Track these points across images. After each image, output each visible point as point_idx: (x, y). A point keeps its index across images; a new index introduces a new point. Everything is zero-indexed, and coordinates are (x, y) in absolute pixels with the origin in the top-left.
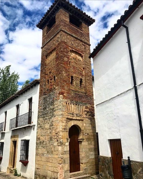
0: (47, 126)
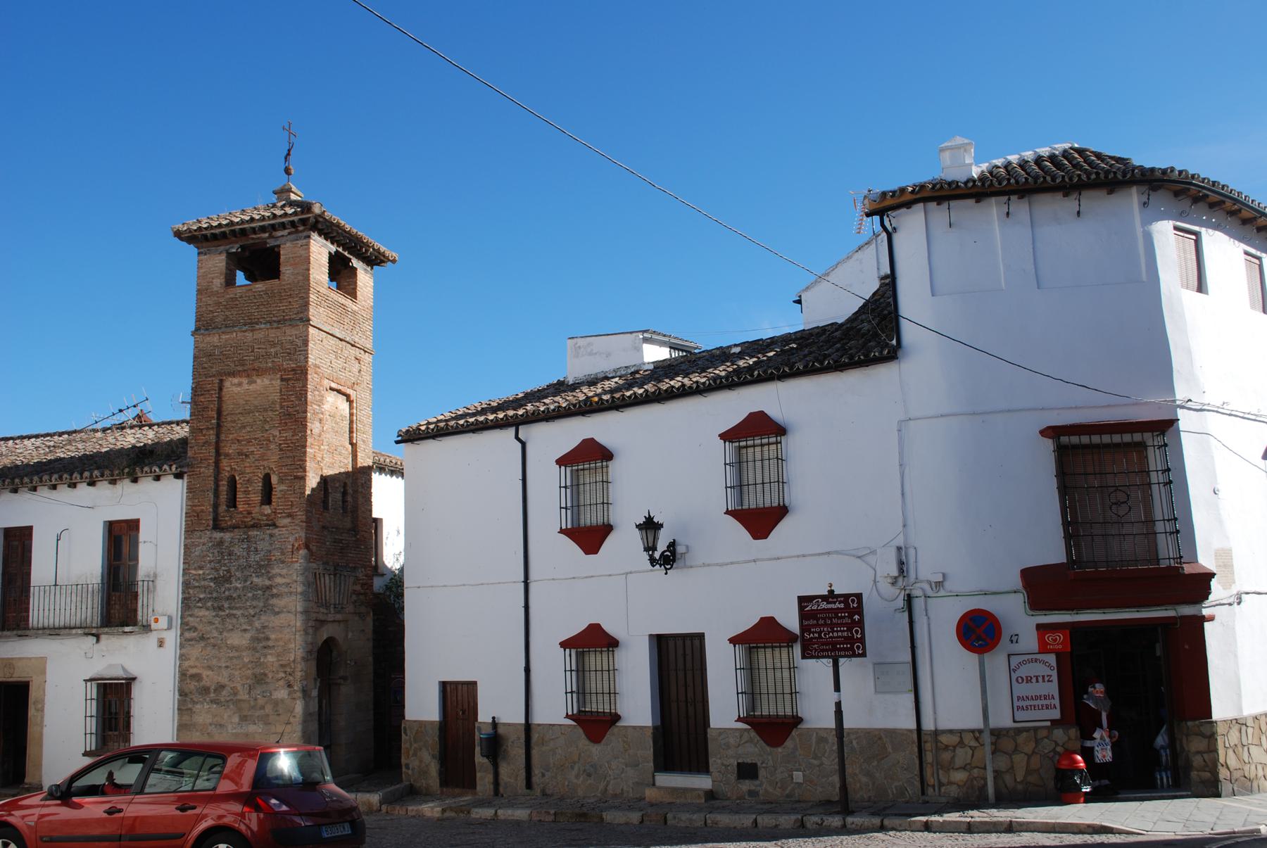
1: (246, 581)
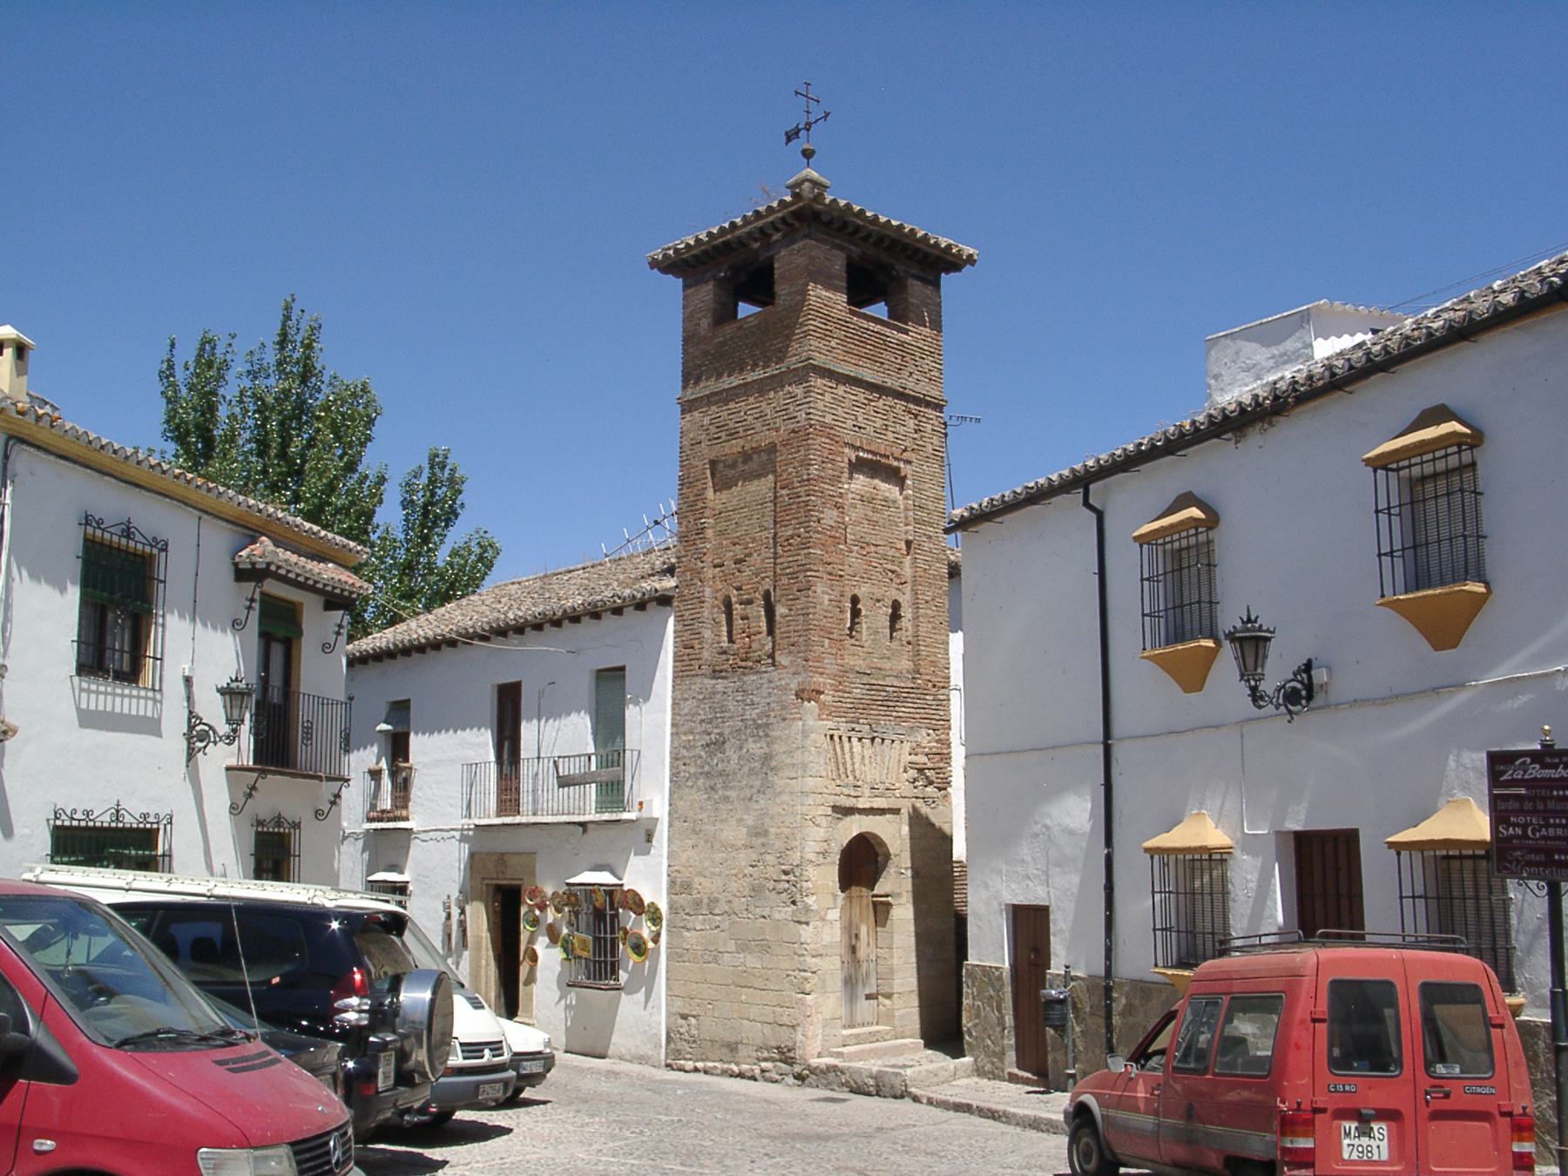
0: (734, 833)
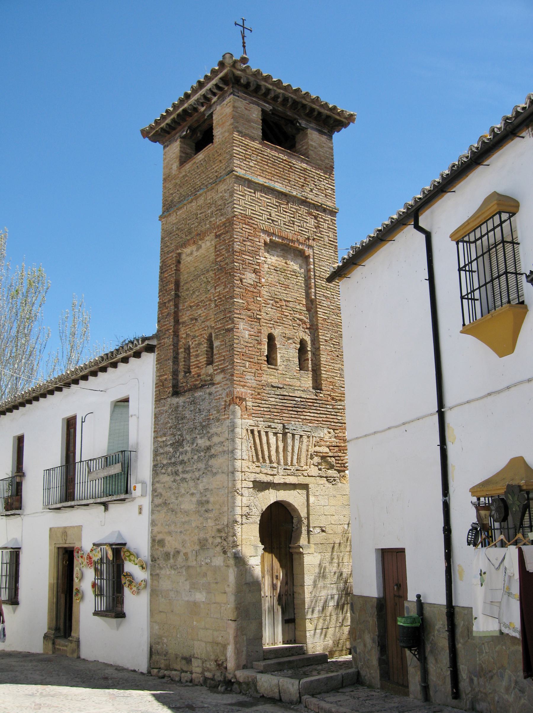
0: (188, 504)
1: (193, 444)
